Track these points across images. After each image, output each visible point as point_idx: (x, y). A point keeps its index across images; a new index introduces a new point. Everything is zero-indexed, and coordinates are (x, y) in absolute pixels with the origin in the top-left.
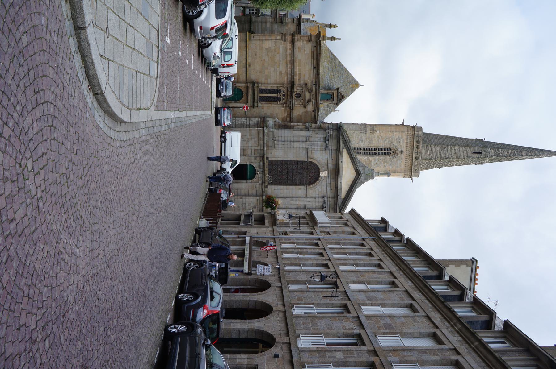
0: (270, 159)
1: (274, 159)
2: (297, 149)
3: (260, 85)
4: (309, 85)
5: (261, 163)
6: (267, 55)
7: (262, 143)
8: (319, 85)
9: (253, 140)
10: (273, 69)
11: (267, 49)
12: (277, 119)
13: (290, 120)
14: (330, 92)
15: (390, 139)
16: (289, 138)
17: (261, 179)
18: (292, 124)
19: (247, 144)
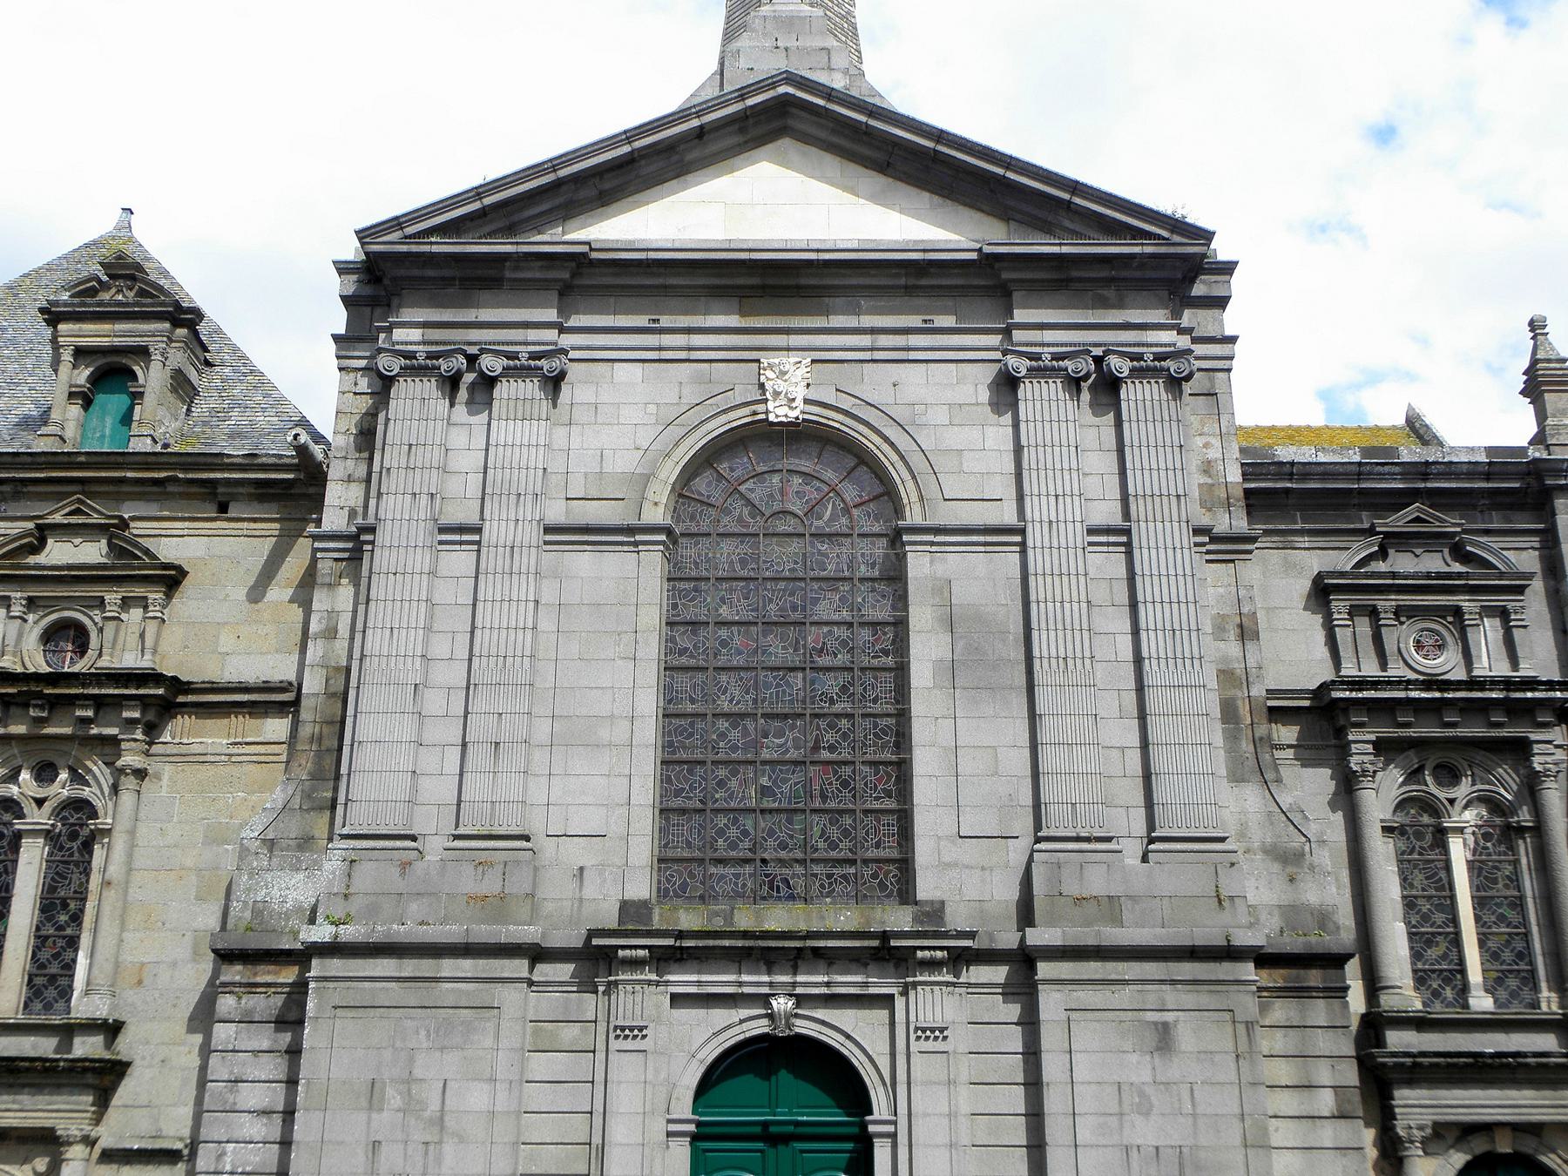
0: (641, 888)
1: (642, 850)
2: (547, 624)
5: (684, 980)
7: (467, 966)
9: (431, 1067)
13: (281, 708)
16: (434, 702)
17: (848, 981)
18: (313, 684)
19: (462, 1139)
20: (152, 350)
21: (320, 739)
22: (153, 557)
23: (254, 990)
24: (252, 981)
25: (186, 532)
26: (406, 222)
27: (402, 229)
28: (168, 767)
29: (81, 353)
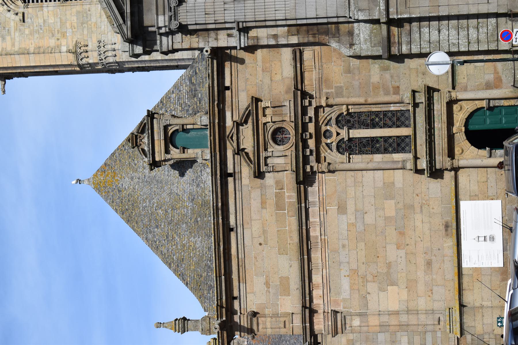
3: (410, 165)
4: (246, 171)
6: (389, 265)
8: (214, 174)
10: (369, 219)
11: (393, 284)
12: (346, 51)
14: (175, 154)
15: (27, 32)
18: (294, 40)
20: (165, 124)
21: (314, 34)
22: (249, 106)
23: (400, 42)
24: (397, 43)
25: (237, 100)
26: (118, 23)
27: (121, 25)
28: (324, 91)
29: (167, 151)
